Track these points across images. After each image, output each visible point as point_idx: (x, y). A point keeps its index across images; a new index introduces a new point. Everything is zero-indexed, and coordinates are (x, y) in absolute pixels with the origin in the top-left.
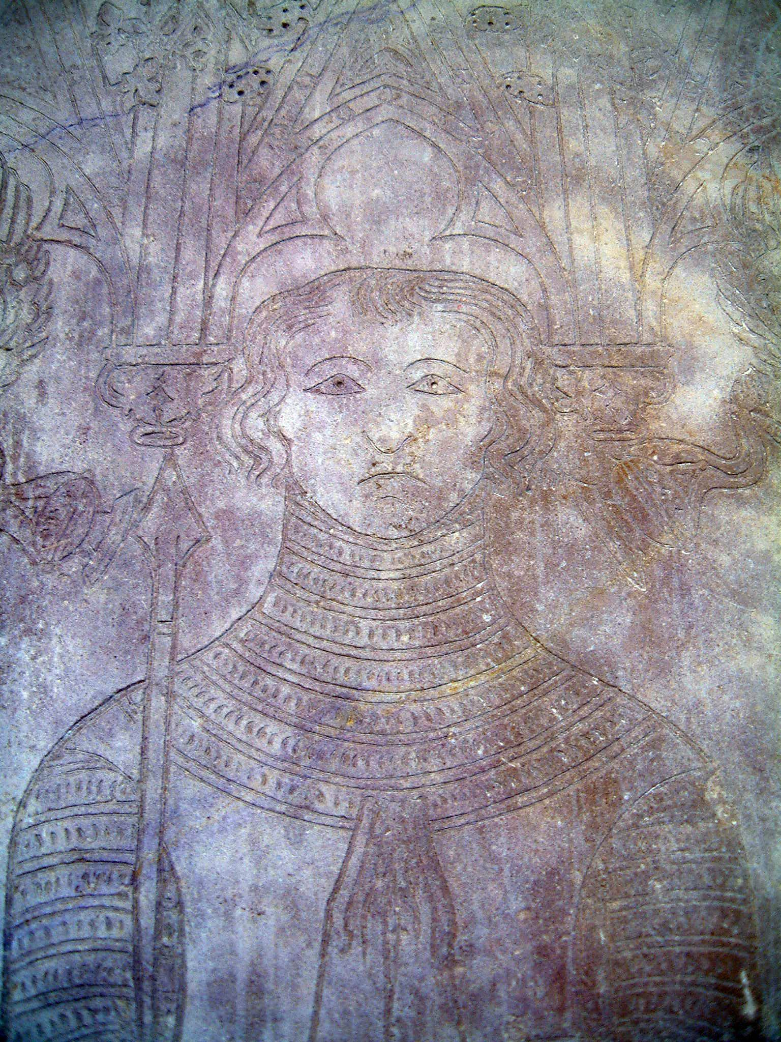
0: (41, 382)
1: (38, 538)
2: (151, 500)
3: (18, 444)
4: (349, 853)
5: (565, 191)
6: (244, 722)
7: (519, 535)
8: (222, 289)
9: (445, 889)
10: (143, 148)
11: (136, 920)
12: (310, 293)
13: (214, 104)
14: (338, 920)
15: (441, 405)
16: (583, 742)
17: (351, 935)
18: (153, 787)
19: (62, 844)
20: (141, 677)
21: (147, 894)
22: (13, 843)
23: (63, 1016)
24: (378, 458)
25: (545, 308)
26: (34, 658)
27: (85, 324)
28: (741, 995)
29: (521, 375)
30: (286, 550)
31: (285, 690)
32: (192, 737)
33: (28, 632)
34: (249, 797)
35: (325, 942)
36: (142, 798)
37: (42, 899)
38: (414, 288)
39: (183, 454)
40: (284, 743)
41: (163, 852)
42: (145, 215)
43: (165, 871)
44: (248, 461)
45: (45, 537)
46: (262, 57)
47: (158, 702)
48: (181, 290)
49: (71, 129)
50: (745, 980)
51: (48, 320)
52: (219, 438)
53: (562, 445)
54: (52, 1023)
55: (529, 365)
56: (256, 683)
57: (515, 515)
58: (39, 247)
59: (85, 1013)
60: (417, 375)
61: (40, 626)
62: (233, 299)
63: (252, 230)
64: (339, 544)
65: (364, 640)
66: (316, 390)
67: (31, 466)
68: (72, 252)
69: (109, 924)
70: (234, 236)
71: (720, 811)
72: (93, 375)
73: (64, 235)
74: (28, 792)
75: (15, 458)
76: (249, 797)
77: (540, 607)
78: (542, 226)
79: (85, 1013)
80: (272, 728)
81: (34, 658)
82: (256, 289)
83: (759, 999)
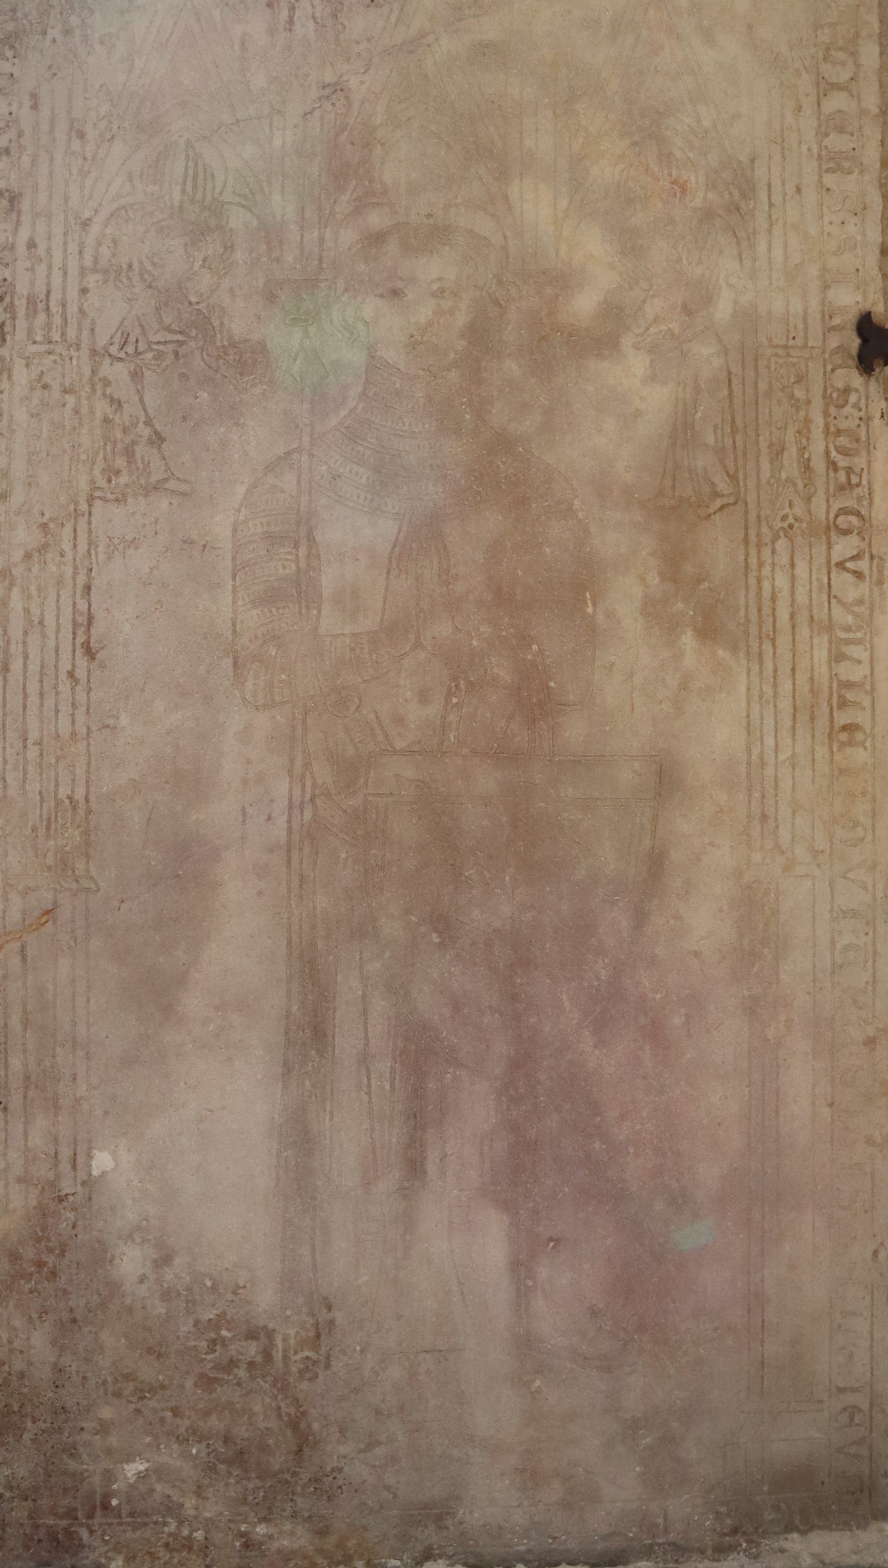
0: (231, 288)
1: (238, 376)
2: (297, 355)
3: (222, 324)
4: (399, 532)
5: (521, 174)
6: (348, 469)
7: (484, 375)
8: (328, 234)
9: (445, 548)
10: (278, 143)
11: (297, 565)
12: (377, 239)
13: (317, 113)
14: (394, 564)
15: (447, 304)
16: (514, 478)
17: (400, 570)
18: (304, 499)
19: (259, 530)
20: (296, 446)
21: (303, 551)
22: (235, 530)
23: (262, 611)
24: (415, 333)
25: (505, 248)
26: (240, 437)
27: (253, 255)
28: (587, 603)
29: (490, 288)
30: (368, 382)
31: (368, 452)
32: (322, 477)
33: (237, 424)
34: (351, 504)
35: (388, 573)
36: (299, 506)
37: (252, 556)
38: (436, 235)
39: (312, 330)
40: (368, 478)
41: (310, 532)
42: (283, 187)
43: (311, 540)
44: (347, 335)
45: (241, 375)
46: (344, 78)
47: (305, 458)
48: (306, 235)
49: (232, 127)
50: (588, 596)
51: (232, 251)
52: (331, 321)
53: (510, 327)
54: (258, 614)
55: (494, 281)
56: (353, 449)
57: (483, 364)
58: (222, 206)
59: (273, 609)
60: (435, 287)
61: (242, 421)
62: (336, 241)
63: (345, 198)
64: (394, 378)
65: (406, 428)
66: (382, 296)
67: (230, 338)
68: (242, 210)
69: (284, 567)
70: (335, 202)
71: (580, 515)
72: (261, 284)
73: (237, 199)
74: (241, 505)
75: (221, 332)
76: (351, 504)
77: (494, 411)
78: (506, 198)
79: (273, 609)
80: (361, 470)
81: (240, 437)
82: (348, 236)
83: (594, 605)
